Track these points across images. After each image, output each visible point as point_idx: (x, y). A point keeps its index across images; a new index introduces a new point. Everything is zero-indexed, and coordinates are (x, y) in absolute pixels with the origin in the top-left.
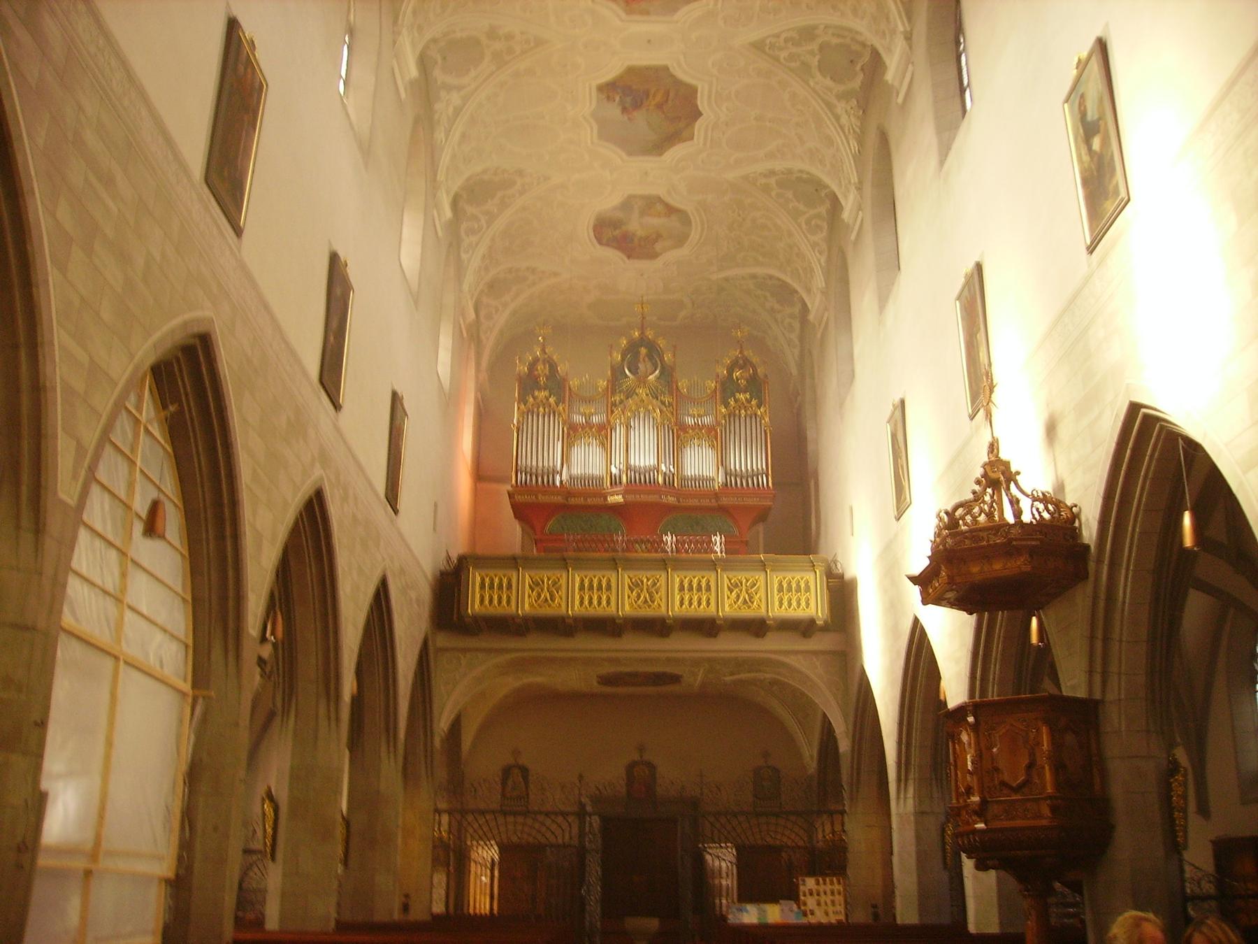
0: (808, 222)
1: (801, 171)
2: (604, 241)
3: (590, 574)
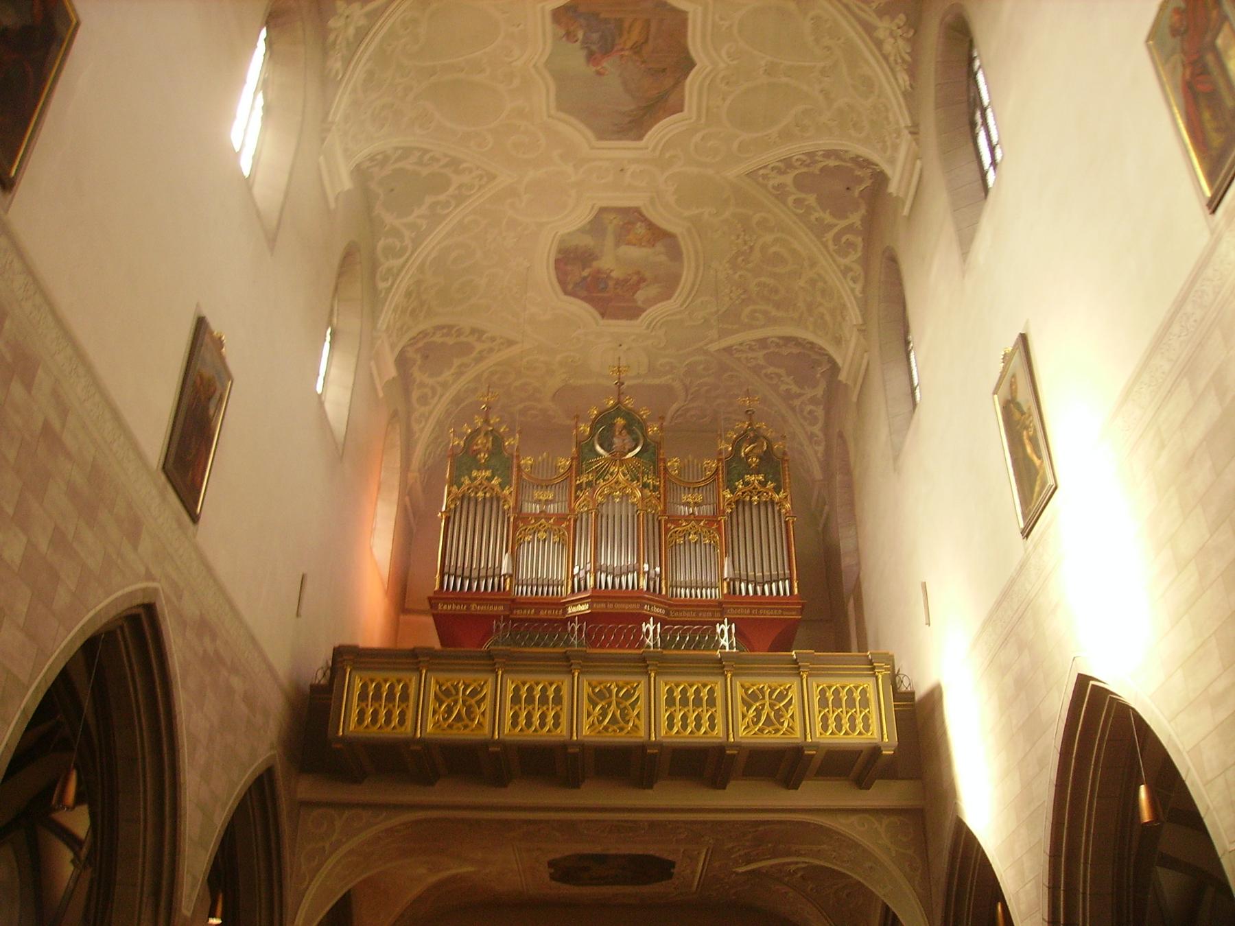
0: (837, 239)
1: (828, 154)
2: (570, 287)
3: (530, 679)
